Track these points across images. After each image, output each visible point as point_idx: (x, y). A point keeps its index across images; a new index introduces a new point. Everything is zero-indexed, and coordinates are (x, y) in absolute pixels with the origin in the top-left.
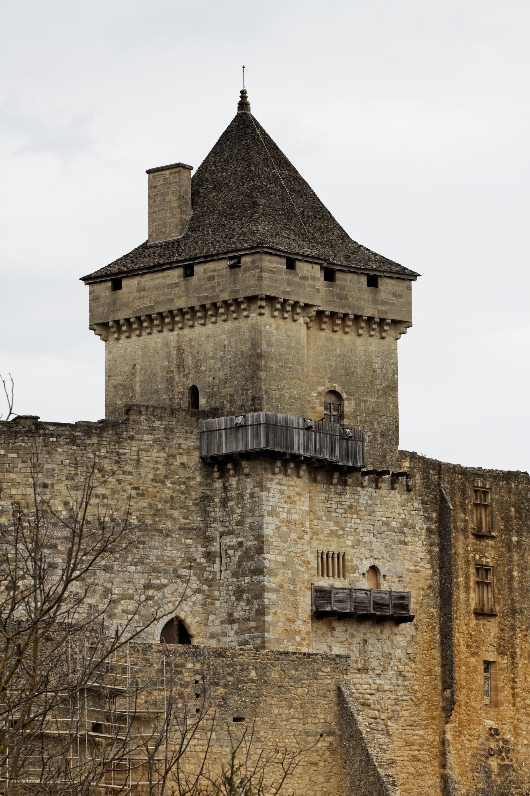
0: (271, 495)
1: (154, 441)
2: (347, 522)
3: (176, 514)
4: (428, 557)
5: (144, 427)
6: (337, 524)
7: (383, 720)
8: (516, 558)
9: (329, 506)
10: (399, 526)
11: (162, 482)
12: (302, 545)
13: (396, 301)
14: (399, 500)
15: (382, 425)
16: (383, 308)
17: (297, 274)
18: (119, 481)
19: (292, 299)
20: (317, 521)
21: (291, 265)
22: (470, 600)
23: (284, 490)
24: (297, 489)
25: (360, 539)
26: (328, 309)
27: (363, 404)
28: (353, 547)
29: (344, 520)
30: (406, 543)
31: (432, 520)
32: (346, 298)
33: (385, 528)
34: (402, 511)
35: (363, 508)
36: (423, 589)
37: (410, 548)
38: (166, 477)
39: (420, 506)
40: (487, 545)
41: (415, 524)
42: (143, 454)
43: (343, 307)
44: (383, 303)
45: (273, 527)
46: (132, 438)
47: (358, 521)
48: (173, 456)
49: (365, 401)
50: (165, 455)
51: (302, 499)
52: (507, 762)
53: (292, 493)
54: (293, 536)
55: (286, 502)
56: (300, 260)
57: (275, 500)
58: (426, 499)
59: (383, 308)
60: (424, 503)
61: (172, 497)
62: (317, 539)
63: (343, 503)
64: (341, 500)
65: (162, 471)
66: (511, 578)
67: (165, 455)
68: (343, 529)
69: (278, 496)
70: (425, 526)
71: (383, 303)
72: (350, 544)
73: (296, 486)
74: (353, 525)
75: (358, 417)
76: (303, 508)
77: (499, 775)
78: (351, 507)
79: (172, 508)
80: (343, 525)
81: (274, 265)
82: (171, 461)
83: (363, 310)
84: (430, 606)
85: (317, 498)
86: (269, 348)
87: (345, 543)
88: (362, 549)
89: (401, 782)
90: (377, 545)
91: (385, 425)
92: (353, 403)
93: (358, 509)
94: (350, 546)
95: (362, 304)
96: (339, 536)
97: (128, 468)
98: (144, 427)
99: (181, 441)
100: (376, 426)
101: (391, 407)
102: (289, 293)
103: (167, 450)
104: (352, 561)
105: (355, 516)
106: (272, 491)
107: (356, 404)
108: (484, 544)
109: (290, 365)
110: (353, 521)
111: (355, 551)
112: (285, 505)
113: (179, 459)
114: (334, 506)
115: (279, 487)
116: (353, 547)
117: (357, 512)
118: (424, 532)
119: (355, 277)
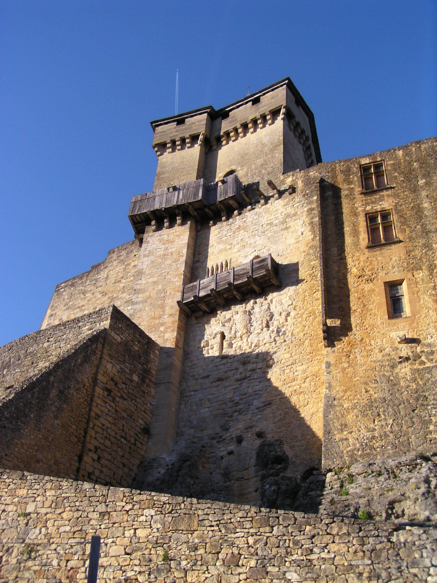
0: (149, 245)
1: (118, 263)
3: (124, 295)
4: (309, 228)
5: (115, 258)
6: (225, 242)
7: (261, 368)
8: (424, 193)
10: (281, 220)
11: (120, 281)
13: (273, 100)
14: (283, 204)
15: (268, 169)
16: (263, 109)
18: (93, 294)
21: (181, 122)
22: (360, 240)
24: (178, 233)
25: (245, 244)
27: (253, 166)
28: (239, 251)
30: (287, 228)
31: (313, 202)
32: (236, 120)
33: (269, 226)
34: (284, 210)
35: (250, 224)
36: (304, 252)
37: (291, 230)
38: (122, 278)
39: (303, 199)
40: (383, 196)
41: (297, 212)
42: (111, 272)
45: (149, 262)
46: (106, 268)
47: (245, 233)
48: (129, 264)
50: (124, 266)
51: (181, 237)
52: (428, 364)
53: (171, 237)
54: (168, 262)
56: (187, 118)
58: (307, 192)
59: (263, 109)
60: (304, 196)
61: (124, 287)
65: (121, 275)
66: (418, 210)
67: (124, 266)
68: (231, 244)
69: (157, 243)
70: (306, 209)
71: (263, 107)
73: (176, 232)
75: (249, 175)
77: (414, 380)
79: (122, 293)
82: (127, 267)
83: (248, 118)
84: (311, 261)
88: (247, 250)
89: (279, 418)
90: (260, 241)
91: (271, 168)
92: (245, 169)
97: (101, 284)
98: (115, 258)
99: (136, 254)
100: (263, 171)
101: (277, 155)
103: (126, 263)
104: (237, 260)
105: (243, 231)
106: (151, 242)
107: (248, 169)
108: (378, 196)
111: (240, 253)
112: (163, 246)
113: (132, 265)
114: (225, 233)
115: (159, 237)
116: (239, 251)
117: (244, 228)
118: (304, 214)
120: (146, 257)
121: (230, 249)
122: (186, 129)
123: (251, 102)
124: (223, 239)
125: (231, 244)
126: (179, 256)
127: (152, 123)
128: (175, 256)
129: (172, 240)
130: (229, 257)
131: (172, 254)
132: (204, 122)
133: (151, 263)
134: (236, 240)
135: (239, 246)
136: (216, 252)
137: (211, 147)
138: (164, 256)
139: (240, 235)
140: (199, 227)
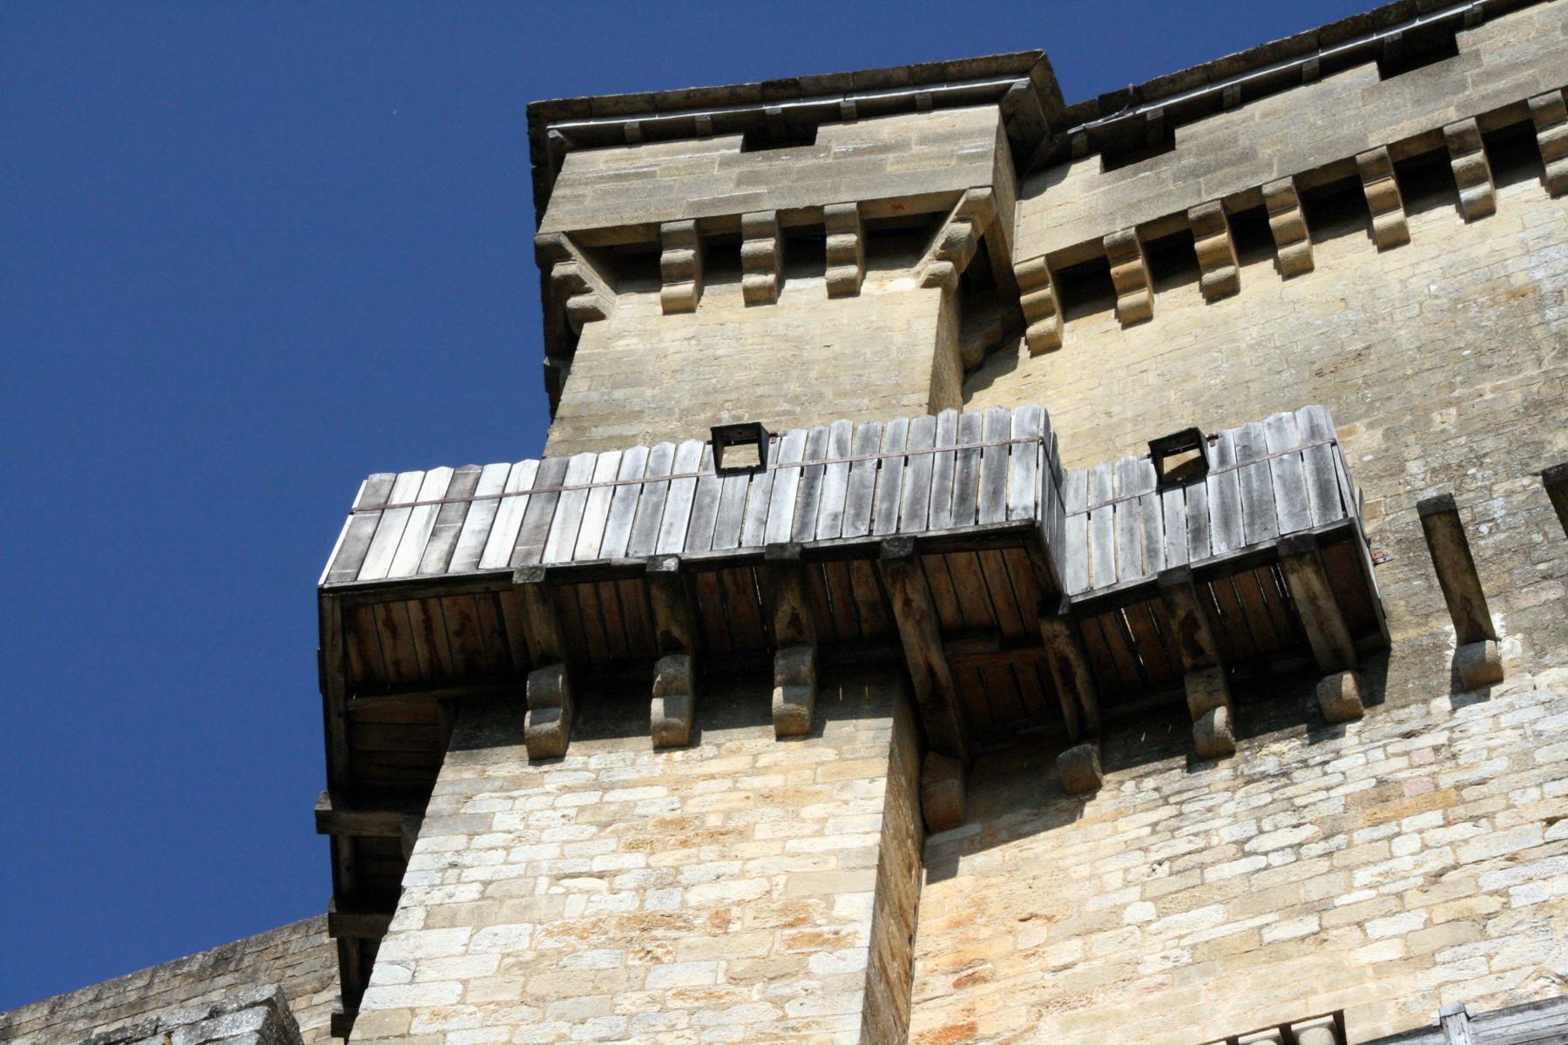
2: (1349, 869)
6: (1253, 899)
9: (1181, 846)
12: (779, 1002)
17: (827, 149)
19: (764, 212)
20: (1077, 943)
23: (628, 806)
24: (775, 781)
26: (1118, 228)
29: (1324, 864)
43: (1221, 184)
44: (1491, 75)
47: (1462, 830)
49: (1457, 402)
51: (812, 811)
55: (633, 847)
56: (835, 116)
57: (521, 853)
62: (1067, 1026)
63: (1298, 802)
64: (1290, 791)
71: (1491, 75)
72: (1393, 951)
74: (1404, 864)
75: (1414, 467)
76: (820, 845)
78: (1384, 791)
80: (1315, 891)
81: (650, 160)
85: (1070, 851)
86: (619, 394)
87: (1336, 967)
93: (1446, 781)
94: (1380, 969)
95: (1346, 131)
96: (1277, 952)
102: (746, 199)
105: (1435, 817)
106: (503, 820)
109: (786, 406)
110: (1417, 840)
111: (1438, 974)
112: (637, 859)
114: (1225, 833)
115: (593, 797)
119: (1301, 92)
120: (452, 922)
121: (1319, 937)
122: (824, 171)
123: (1371, 68)
124: (1211, 875)
125: (1320, 907)
126: (792, 943)
127: (538, 116)
128: (755, 941)
129: (714, 821)
130: (1323, 1004)
131: (721, 920)
132: (989, 143)
133: (503, 970)
134: (1362, 876)
135: (1414, 920)
136: (1152, 965)
137: (1017, 325)
138: (645, 933)
139: (1406, 846)
140: (950, 790)
